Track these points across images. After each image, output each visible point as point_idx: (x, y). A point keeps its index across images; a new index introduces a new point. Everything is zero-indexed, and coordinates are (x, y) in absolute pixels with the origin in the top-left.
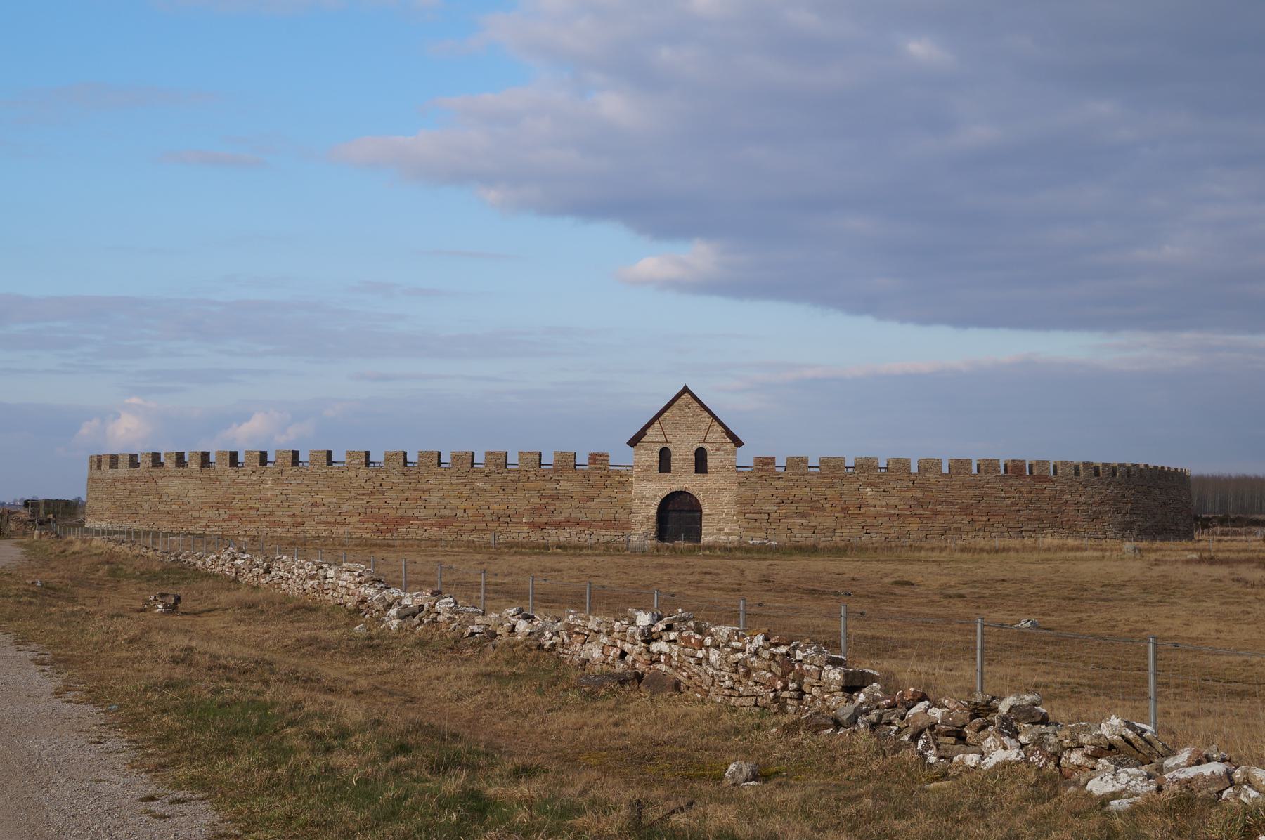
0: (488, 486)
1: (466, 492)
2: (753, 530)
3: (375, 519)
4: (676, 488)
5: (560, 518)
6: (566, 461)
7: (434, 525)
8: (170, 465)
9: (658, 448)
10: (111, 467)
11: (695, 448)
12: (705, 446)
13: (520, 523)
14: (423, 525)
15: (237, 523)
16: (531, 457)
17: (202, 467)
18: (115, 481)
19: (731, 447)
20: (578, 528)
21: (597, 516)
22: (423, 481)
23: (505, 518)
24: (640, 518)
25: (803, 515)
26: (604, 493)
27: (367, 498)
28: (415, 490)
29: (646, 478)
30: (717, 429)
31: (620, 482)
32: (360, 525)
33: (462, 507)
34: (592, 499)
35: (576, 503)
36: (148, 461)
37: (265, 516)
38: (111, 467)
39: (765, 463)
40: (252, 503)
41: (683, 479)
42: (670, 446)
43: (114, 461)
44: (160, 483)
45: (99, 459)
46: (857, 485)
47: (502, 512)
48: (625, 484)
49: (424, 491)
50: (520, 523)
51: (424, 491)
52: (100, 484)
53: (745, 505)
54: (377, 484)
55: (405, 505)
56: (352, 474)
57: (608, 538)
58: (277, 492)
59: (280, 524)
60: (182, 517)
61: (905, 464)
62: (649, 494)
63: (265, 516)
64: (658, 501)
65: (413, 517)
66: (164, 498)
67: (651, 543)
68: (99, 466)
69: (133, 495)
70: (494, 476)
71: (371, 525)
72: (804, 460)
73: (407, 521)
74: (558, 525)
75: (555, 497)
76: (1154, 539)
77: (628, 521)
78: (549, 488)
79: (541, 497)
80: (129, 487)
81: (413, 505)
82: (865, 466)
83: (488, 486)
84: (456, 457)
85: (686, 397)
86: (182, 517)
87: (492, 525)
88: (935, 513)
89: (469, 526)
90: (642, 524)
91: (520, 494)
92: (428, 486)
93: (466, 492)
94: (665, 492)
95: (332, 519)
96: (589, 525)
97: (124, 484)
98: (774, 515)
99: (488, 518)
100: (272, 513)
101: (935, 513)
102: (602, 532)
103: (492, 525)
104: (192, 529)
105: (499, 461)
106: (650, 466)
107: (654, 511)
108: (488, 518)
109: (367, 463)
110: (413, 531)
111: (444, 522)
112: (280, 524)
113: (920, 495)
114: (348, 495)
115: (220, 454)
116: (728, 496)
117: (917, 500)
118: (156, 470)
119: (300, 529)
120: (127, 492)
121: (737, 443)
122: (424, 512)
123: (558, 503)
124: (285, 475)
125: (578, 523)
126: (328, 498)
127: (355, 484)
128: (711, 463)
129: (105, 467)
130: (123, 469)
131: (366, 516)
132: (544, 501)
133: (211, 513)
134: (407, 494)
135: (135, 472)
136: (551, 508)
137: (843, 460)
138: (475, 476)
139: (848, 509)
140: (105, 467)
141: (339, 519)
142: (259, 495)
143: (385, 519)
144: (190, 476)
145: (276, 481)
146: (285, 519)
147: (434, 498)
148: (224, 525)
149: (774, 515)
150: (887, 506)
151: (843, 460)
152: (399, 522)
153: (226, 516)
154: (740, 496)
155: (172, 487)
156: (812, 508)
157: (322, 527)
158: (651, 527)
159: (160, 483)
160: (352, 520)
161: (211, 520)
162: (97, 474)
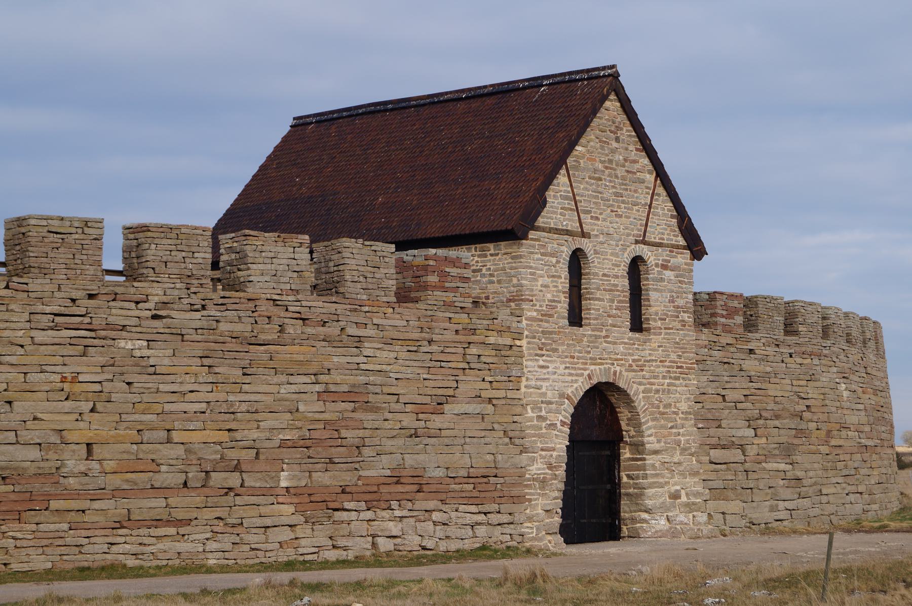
0: (160, 356)
5: (378, 469)
9: (566, 253)
13: (269, 492)
19: (683, 258)
21: (461, 461)
23: (222, 479)
24: (537, 468)
25: (787, 451)
26: (470, 384)
30: (664, 206)
31: (497, 348)
33: (81, 433)
35: (408, 421)
42: (586, 245)
47: (211, 455)
74: (374, 498)
75: (356, 397)
83: (160, 356)
85: (612, 104)
89: (113, 508)
90: (543, 482)
91: (266, 388)
99: (169, 477)
102: (467, 514)
107: (560, 443)
108: (169, 477)
116: (682, 398)
123: (369, 419)
128: (657, 302)
138: (118, 314)
149: (752, 451)
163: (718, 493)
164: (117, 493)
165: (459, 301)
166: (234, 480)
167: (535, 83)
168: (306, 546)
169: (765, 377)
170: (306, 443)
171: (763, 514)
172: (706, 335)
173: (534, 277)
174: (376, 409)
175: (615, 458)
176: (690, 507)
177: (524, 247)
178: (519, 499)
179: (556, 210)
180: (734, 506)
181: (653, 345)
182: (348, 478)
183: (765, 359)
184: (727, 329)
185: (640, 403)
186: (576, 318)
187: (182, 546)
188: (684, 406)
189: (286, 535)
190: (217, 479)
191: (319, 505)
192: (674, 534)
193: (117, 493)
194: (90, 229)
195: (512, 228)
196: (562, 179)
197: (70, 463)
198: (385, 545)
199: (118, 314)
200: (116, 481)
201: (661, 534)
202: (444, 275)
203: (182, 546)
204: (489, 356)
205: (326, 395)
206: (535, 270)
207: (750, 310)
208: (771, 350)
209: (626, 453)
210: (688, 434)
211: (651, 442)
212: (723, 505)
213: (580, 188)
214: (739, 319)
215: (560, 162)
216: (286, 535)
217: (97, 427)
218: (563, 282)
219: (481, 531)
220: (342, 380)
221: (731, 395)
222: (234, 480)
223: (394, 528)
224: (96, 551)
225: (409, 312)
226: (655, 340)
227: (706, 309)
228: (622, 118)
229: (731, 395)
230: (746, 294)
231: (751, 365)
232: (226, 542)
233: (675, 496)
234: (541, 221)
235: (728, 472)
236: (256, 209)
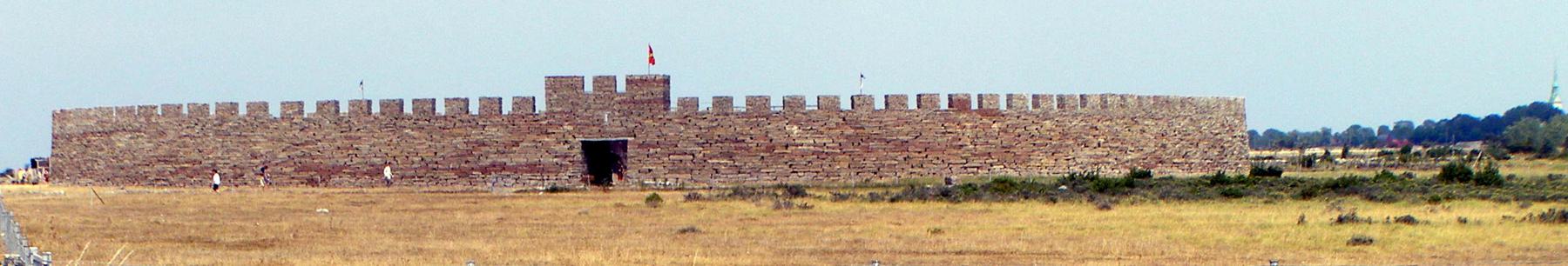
2: (678, 171)
5: (486, 162)
6: (492, 105)
21: (522, 160)
34: (517, 144)
40: (195, 156)
46: (782, 124)
55: (337, 155)
61: (835, 100)
65: (345, 166)
72: (729, 100)
76: (1343, 179)
78: (475, 135)
82: (793, 104)
83: (415, 134)
84: (384, 105)
88: (869, 150)
101: (869, 150)
103: (421, 172)
105: (425, 107)
109: (301, 112)
113: (850, 131)
114: (285, 145)
117: (847, 137)
122: (356, 160)
125: (504, 167)
133: (159, 167)
134: (339, 143)
137: (767, 100)
139: (771, 149)
145: (217, 133)
147: (365, 147)
150: (815, 145)
151: (767, 100)
160: (288, 170)
220: (473, 139)
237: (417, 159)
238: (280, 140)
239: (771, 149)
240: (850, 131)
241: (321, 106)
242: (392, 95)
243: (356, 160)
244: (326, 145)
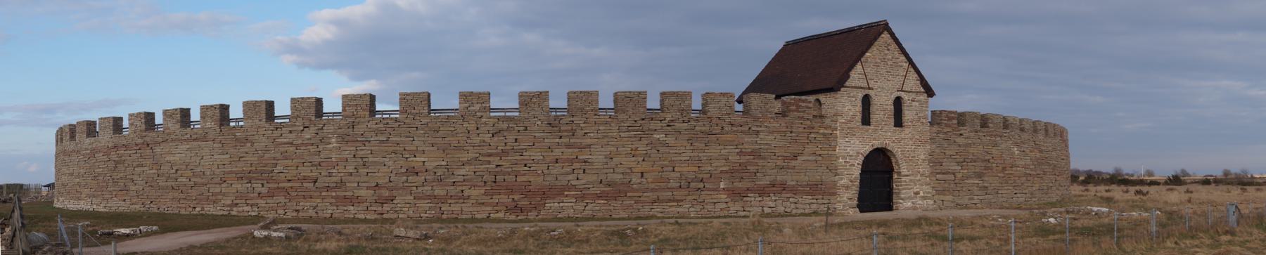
0: (671, 140)
1: (642, 148)
3: (510, 190)
4: (877, 144)
5: (764, 181)
7: (599, 197)
8: (175, 127)
9: (860, 96)
10: (88, 136)
11: (893, 97)
12: (903, 95)
13: (717, 190)
14: (583, 197)
15: (282, 199)
16: (724, 100)
17: (221, 125)
18: (94, 152)
19: (923, 97)
20: (785, 195)
21: (804, 179)
22: (579, 133)
24: (845, 181)
25: (979, 176)
27: (496, 160)
28: (569, 146)
29: (850, 133)
30: (913, 76)
31: (824, 134)
32: (487, 200)
33: (638, 169)
34: (795, 157)
36: (141, 124)
37: (328, 189)
38: (88, 136)
39: (950, 115)
40: (306, 171)
41: (883, 135)
43: (90, 128)
44: (158, 150)
45: (72, 129)
47: (691, 176)
48: (830, 139)
49: (581, 148)
50: (717, 190)
51: (581, 148)
52: (74, 157)
53: (935, 162)
54: (511, 138)
55: (556, 170)
56: (472, 127)
57: (814, 206)
58: (346, 155)
59: (354, 201)
60: (194, 193)
62: (852, 149)
63: (328, 189)
64: (861, 159)
66: (165, 169)
67: (854, 214)
68: (72, 137)
69: (121, 167)
70: (678, 125)
71: (504, 199)
73: (557, 192)
74: (762, 192)
75: (756, 154)
77: (835, 184)
78: (748, 142)
79: (741, 153)
80: (114, 157)
81: (568, 169)
83: (671, 140)
86: (194, 193)
87: (679, 194)
91: (714, 151)
92: (589, 141)
93: (642, 148)
94: (867, 149)
95: (440, 192)
96: (795, 191)
97: (107, 154)
98: (959, 176)
99: (673, 184)
100: (341, 184)
103: (679, 194)
104: (210, 209)
106: (853, 116)
107: (857, 172)
110: (569, 206)
111: (615, 192)
112: (354, 201)
113: (1038, 155)
114: (464, 157)
115: (249, 106)
116: (922, 153)
118: (151, 134)
119: (386, 207)
120: (111, 164)
121: (930, 92)
122: (585, 179)
123: (761, 162)
124: (360, 129)
125: (784, 187)
126: (432, 160)
127: (476, 140)
128: (908, 115)
129: (81, 136)
130: (105, 138)
131: (495, 187)
132: (744, 159)
133: (240, 186)
134: (557, 153)
135: (117, 139)
136: (752, 169)
138: (653, 125)
139: (1004, 169)
140: (81, 136)
141: (453, 191)
142: (317, 159)
143: (526, 191)
144: (204, 138)
145: (344, 139)
146: (363, 193)
147: (597, 157)
148: (262, 202)
149: (959, 176)
152: (547, 193)
153: (264, 190)
154: (932, 153)
155: (178, 154)
156: (986, 168)
157: (424, 204)
158: (854, 193)
159: (158, 150)
160: (474, 193)
161: (239, 195)
162: (69, 145)
163: (939, 193)
164: (653, 190)
165: (806, 116)
166: (701, 185)
167: (860, 27)
168: (732, 210)
169: (967, 145)
170: (732, 172)
171: (965, 201)
172: (935, 128)
173: (844, 106)
174: (764, 158)
175: (892, 177)
176: (924, 198)
177: (839, 95)
178: (834, 194)
179: (856, 77)
180: (949, 198)
181: (906, 133)
182: (749, 185)
183: (968, 138)
184: (947, 126)
185: (899, 155)
186: (866, 120)
187: (680, 210)
188: (922, 157)
189: (724, 206)
190: (693, 185)
191: (737, 194)
192: (915, 208)
193: (653, 190)
194: (688, 95)
195: (833, 89)
196: (859, 66)
197: (634, 180)
198: (767, 210)
199: (653, 125)
200: (653, 186)
201: (908, 209)
202: (798, 106)
203: (680, 210)
204: (819, 138)
205: (741, 153)
206: (845, 104)
207: (962, 119)
208: (972, 134)
209: (895, 176)
210: (925, 168)
211: (904, 171)
212: (942, 197)
213: (868, 70)
214: (955, 122)
215: (858, 60)
216: (724, 206)
217: (645, 166)
218: (859, 107)
219: (814, 206)
220: (748, 148)
221: (948, 153)
222: (701, 185)
223: (772, 204)
224: (646, 210)
225: (783, 121)
226: (907, 130)
227: (937, 118)
228: (891, 41)
229: (948, 153)
230: (959, 110)
231: (960, 140)
232: (698, 208)
233: (917, 193)
234: (847, 84)
235: (944, 182)
236: (759, 85)
237: (673, 175)
238: (459, 148)
239: (1004, 169)
240: (1038, 155)
241: (527, 100)
242: (629, 85)
243: (585, 179)
244: (538, 156)
